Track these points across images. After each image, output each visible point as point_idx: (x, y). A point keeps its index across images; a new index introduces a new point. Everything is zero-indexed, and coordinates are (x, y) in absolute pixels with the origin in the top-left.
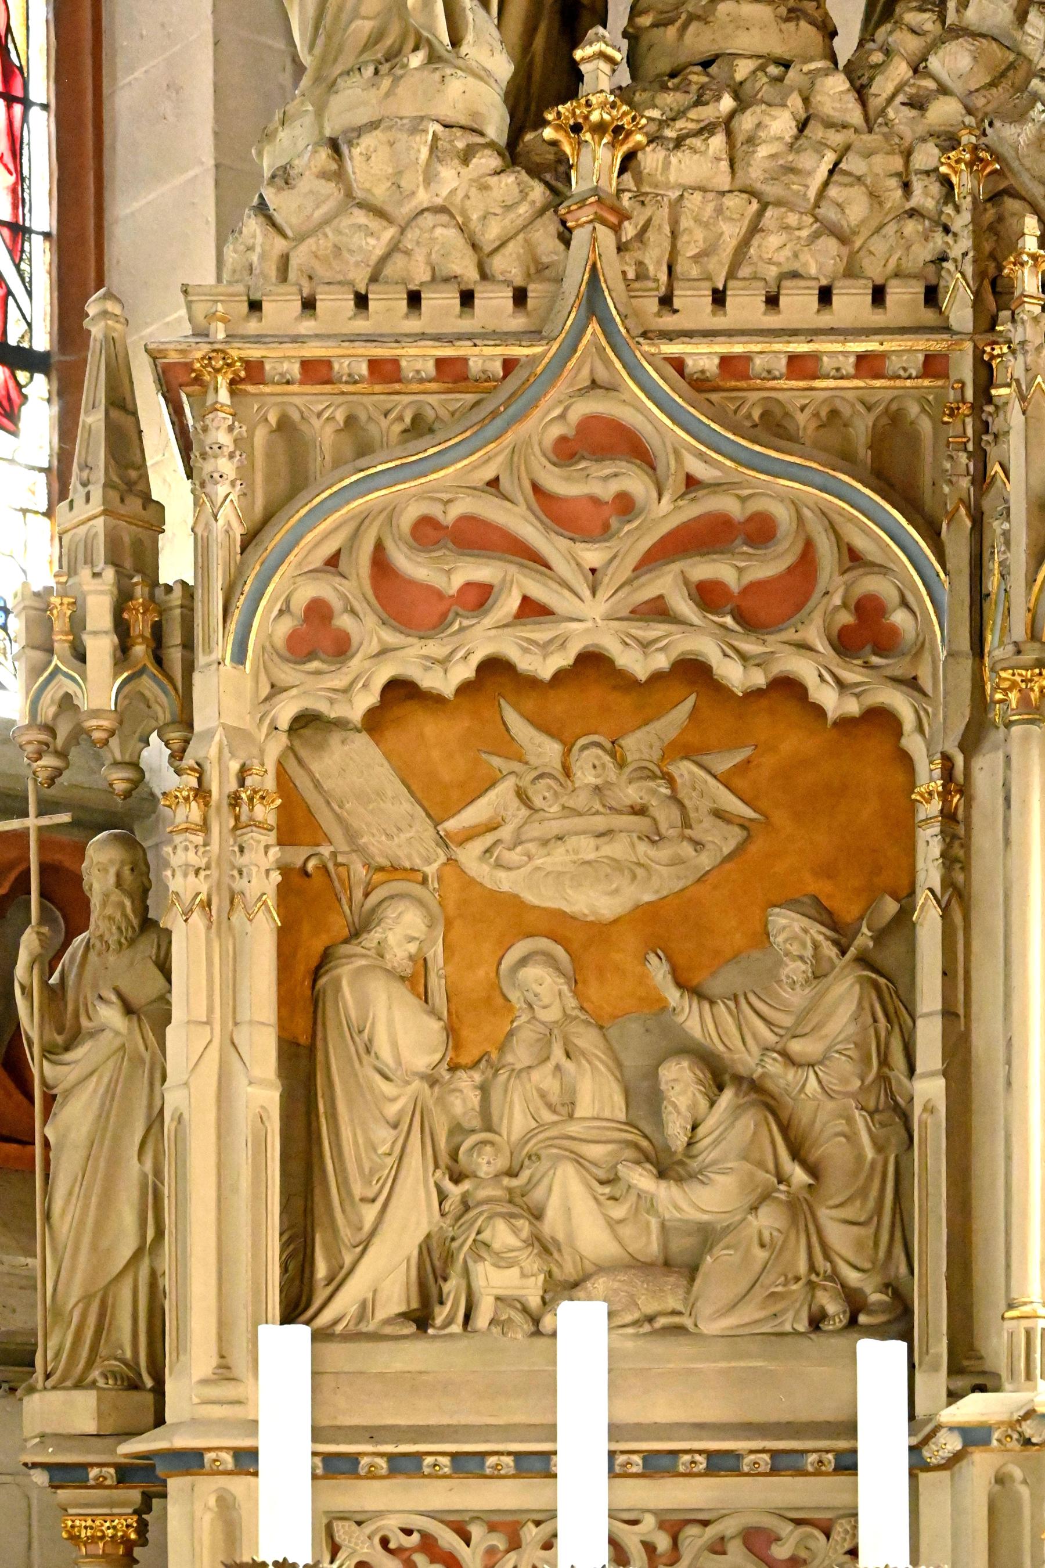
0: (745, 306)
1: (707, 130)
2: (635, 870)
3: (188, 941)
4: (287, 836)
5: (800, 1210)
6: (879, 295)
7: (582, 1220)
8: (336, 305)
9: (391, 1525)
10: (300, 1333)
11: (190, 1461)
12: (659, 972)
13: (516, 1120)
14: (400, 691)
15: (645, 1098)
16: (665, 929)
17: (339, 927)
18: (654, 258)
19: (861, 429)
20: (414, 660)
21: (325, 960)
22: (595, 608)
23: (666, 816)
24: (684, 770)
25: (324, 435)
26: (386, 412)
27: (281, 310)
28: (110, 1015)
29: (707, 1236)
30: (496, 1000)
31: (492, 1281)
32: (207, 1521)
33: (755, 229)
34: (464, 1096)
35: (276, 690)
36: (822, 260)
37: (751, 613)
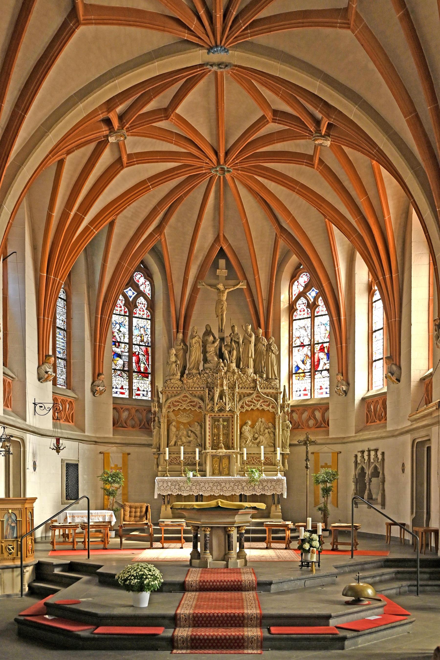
0: (193, 389)
2: (187, 420)
3: (162, 424)
4: (167, 418)
5: (196, 439)
7: (184, 440)
8: (170, 388)
11: (162, 453)
13: (180, 434)
14: (174, 410)
15: (188, 433)
20: (174, 408)
22: (185, 406)
25: (170, 395)
28: (157, 427)
29: (191, 441)
30: (179, 427)
31: (179, 443)
34: (177, 433)
36: (198, 386)
37: (194, 406)
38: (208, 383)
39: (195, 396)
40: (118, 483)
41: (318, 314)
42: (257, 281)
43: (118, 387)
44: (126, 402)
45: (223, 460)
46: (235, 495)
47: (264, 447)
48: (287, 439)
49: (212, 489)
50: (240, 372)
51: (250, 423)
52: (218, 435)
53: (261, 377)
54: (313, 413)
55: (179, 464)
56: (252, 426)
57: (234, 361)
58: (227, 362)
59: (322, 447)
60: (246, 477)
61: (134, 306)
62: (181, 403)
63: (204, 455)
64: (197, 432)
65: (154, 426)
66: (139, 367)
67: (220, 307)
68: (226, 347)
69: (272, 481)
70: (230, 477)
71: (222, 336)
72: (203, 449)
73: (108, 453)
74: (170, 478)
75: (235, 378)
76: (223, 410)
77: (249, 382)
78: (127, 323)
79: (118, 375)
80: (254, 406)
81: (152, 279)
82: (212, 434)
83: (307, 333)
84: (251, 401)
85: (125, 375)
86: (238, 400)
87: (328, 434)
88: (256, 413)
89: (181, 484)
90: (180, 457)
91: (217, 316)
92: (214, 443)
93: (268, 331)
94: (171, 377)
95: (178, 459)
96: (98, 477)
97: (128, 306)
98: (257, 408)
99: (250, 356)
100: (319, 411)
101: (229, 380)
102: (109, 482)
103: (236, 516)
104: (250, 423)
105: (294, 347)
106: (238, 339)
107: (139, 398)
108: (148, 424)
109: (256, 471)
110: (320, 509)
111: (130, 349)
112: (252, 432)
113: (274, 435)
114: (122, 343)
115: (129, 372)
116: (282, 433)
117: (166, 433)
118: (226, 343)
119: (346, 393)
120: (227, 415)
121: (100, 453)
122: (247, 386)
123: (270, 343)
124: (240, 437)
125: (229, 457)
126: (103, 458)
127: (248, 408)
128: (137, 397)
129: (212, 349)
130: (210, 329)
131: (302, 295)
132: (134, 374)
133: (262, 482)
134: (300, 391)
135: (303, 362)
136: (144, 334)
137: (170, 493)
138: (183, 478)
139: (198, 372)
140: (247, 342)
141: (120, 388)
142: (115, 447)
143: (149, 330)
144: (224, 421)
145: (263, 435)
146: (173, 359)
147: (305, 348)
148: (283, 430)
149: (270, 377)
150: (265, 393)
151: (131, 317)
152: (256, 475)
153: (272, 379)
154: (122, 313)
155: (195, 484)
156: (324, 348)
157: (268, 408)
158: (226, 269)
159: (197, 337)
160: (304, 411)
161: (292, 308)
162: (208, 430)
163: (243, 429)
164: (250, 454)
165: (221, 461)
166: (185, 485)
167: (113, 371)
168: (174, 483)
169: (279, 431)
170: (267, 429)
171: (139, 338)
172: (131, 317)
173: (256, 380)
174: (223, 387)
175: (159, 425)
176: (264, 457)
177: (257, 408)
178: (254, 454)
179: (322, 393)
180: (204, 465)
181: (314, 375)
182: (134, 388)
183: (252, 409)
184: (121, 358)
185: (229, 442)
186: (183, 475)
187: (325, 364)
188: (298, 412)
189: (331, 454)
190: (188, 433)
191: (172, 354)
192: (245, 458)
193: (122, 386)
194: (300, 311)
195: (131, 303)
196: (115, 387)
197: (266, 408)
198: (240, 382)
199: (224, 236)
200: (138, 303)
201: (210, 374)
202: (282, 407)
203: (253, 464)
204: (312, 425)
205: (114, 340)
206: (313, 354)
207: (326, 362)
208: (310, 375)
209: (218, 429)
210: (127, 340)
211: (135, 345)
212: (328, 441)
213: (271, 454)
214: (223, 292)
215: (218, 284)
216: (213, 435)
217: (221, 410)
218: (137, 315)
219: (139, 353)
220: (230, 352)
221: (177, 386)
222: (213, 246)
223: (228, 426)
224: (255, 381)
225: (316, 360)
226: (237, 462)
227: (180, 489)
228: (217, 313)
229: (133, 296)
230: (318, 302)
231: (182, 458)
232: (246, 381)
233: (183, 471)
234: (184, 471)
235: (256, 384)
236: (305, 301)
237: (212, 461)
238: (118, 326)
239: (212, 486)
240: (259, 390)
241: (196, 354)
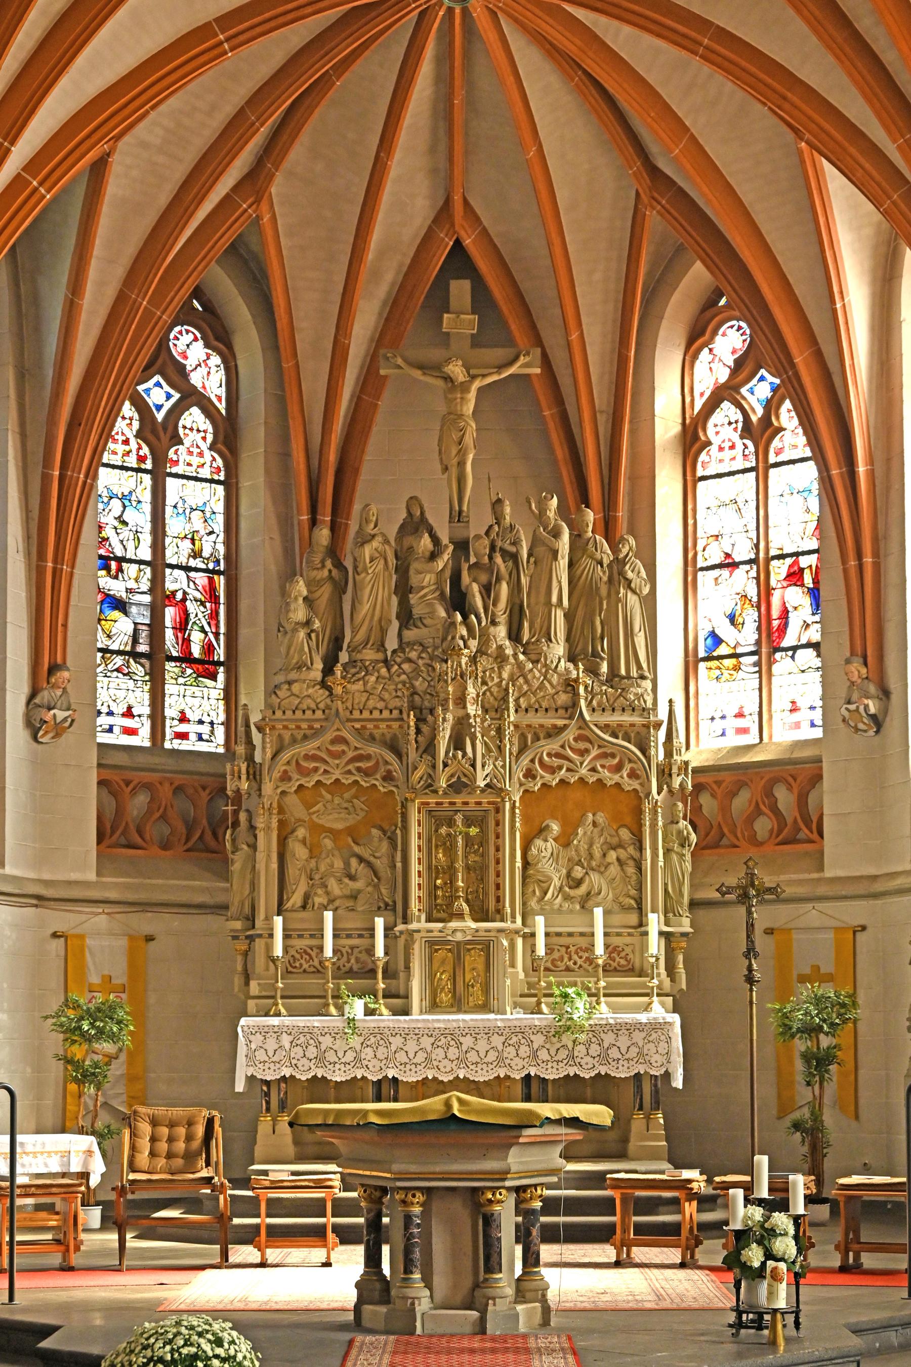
0: (366, 714)
1: (359, 680)
2: (345, 820)
4: (279, 813)
5: (377, 887)
6: (391, 711)
7: (334, 887)
8: (289, 713)
9: (298, 948)
10: (281, 918)
11: (260, 936)
12: (350, 840)
13: (323, 868)
15: (347, 864)
16: (351, 831)
17: (289, 830)
18: (349, 705)
19: (388, 737)
21: (285, 838)
23: (351, 809)
24: (355, 801)
25: (287, 735)
26: (299, 735)
27: (279, 714)
28: (245, 847)
29: (359, 892)
32: (263, 946)
33: (368, 699)
34: (313, 864)
35: (277, 787)
36: (381, 705)
37: (367, 773)
38: (415, 693)
39: (372, 738)
40: (113, 1037)
41: (780, 459)
42: (576, 350)
43: (114, 708)
44: (141, 760)
45: (467, 958)
46: (507, 1077)
47: (606, 913)
48: (681, 884)
49: (428, 1059)
50: (522, 657)
51: (555, 827)
52: (451, 871)
53: (593, 671)
54: (768, 792)
55: (319, 971)
56: (565, 841)
57: (502, 619)
58: (479, 623)
59: (801, 912)
60: (546, 1017)
61: (172, 438)
62: (326, 762)
63: (401, 942)
64: (377, 863)
65: (234, 840)
66: (187, 642)
67: (455, 436)
68: (475, 572)
69: (631, 1028)
70: (492, 1016)
71: (460, 534)
72: (399, 920)
73: (81, 937)
74: (288, 1021)
75: (505, 675)
76: (466, 785)
77: (551, 691)
78: (146, 496)
79: (118, 670)
80: (568, 770)
81: (230, 347)
82: (430, 867)
83: (744, 521)
84: (558, 755)
85: (137, 669)
86: (515, 750)
87: (821, 869)
88: (576, 795)
89: (327, 1041)
90: (321, 948)
91: (446, 469)
92: (436, 897)
93: (615, 518)
94: (293, 675)
95: (313, 954)
96: (46, 1017)
97: (151, 438)
98: (581, 779)
99: (554, 599)
100: (790, 788)
101: (484, 683)
102: (83, 1034)
103: (513, 1151)
104: (555, 827)
105: (702, 569)
106: (516, 543)
107: (185, 746)
108: (215, 834)
109: (579, 994)
110: (797, 1126)
111: (157, 581)
112: (563, 861)
113: (639, 868)
115: (152, 659)
116: (667, 863)
117: (275, 866)
118: (473, 560)
119: (877, 722)
120: (479, 803)
121: (55, 935)
122: (544, 704)
123: (621, 556)
124: (524, 877)
125: (486, 947)
126: (63, 953)
127: (548, 777)
128: (178, 745)
129: (427, 579)
130: (422, 513)
131: (725, 393)
132: (169, 666)
133: (597, 1031)
134: (723, 717)
135: (732, 619)
136: (202, 532)
137: (287, 1072)
138: (333, 1021)
139: (380, 656)
140: (544, 553)
141: (123, 715)
142: (104, 917)
143: (220, 518)
144: (468, 822)
145: (603, 868)
146: (300, 613)
147: (737, 571)
148: (668, 851)
149: (623, 672)
150: (607, 726)
151: (159, 477)
152: (579, 1008)
153: (628, 677)
154: (132, 461)
155: (373, 1040)
156: (802, 570)
157: (616, 778)
158: (473, 313)
159: (379, 538)
160: (741, 784)
161: (692, 440)
162: (414, 854)
163: (534, 851)
164: (559, 934)
165: (458, 961)
166: (339, 1045)
167: (99, 655)
168: (302, 1039)
169: (654, 856)
170: (614, 849)
171: (187, 544)
172: (159, 477)
173: (576, 680)
174: (465, 707)
175: (251, 840)
176: (607, 946)
177: (581, 779)
178: (570, 935)
179: (797, 725)
180: (402, 975)
181: (771, 663)
182: (168, 713)
183: (562, 781)
184: (126, 613)
185: (486, 894)
186: (333, 1010)
187: (807, 626)
188: (719, 792)
189: (831, 935)
190: (347, 864)
191: (296, 598)
192: (541, 950)
193: (130, 708)
194: (721, 449)
195: (160, 429)
196: (104, 710)
197: (610, 778)
198: (520, 688)
199: (466, 202)
200: (184, 427)
201: (420, 662)
202: (665, 773)
203: (568, 969)
204: (767, 835)
205: (102, 552)
206: (765, 591)
207: (810, 619)
208: (758, 664)
209: (450, 850)
210: (145, 553)
212: (822, 890)
213: (630, 934)
214: (464, 388)
215: (448, 361)
216: (432, 870)
217: (458, 786)
218: (179, 469)
219: (185, 593)
220: (487, 590)
221: (313, 706)
222: (428, 239)
223: (482, 840)
224: (570, 685)
225: (775, 613)
226: (513, 965)
227: (320, 1060)
228: (445, 461)
229: (168, 405)
230: (778, 418)
231: (328, 952)
232: (541, 687)
233: (333, 997)
234: (336, 997)
235: (576, 694)
236: (737, 415)
237: (431, 959)
238: (116, 505)
239: (429, 1049)
240: (587, 717)
241: (375, 595)
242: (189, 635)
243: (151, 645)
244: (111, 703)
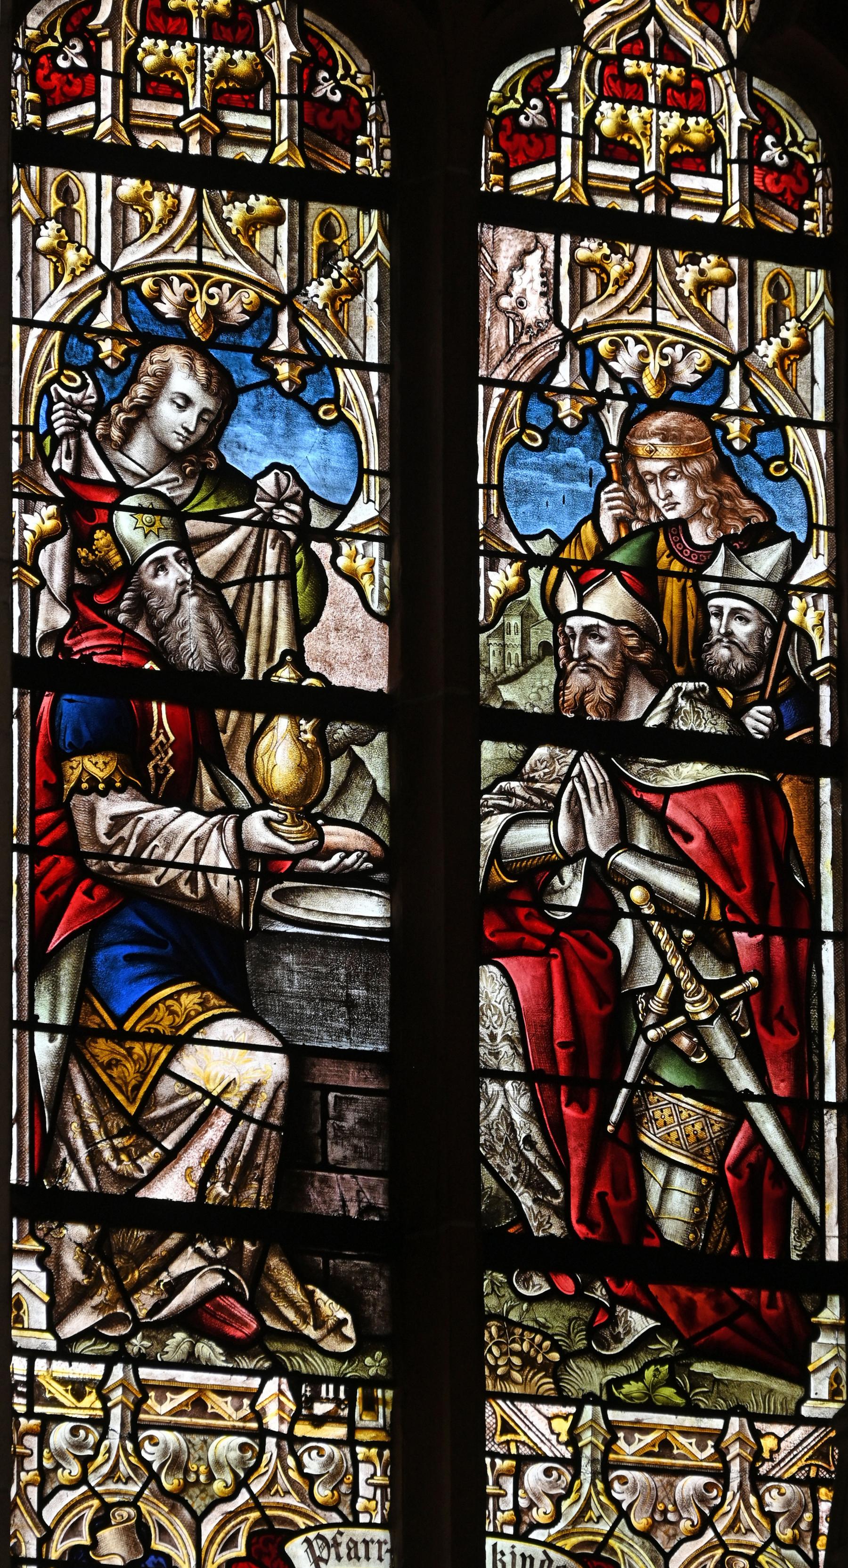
66: (621, 1157)
79: (197, 1320)
114: (271, 700)
210: (352, 650)
211: (524, 729)
219: (602, 879)
238: (181, 391)
242: (634, 1117)
243: (395, 1172)
244: (155, 1512)
